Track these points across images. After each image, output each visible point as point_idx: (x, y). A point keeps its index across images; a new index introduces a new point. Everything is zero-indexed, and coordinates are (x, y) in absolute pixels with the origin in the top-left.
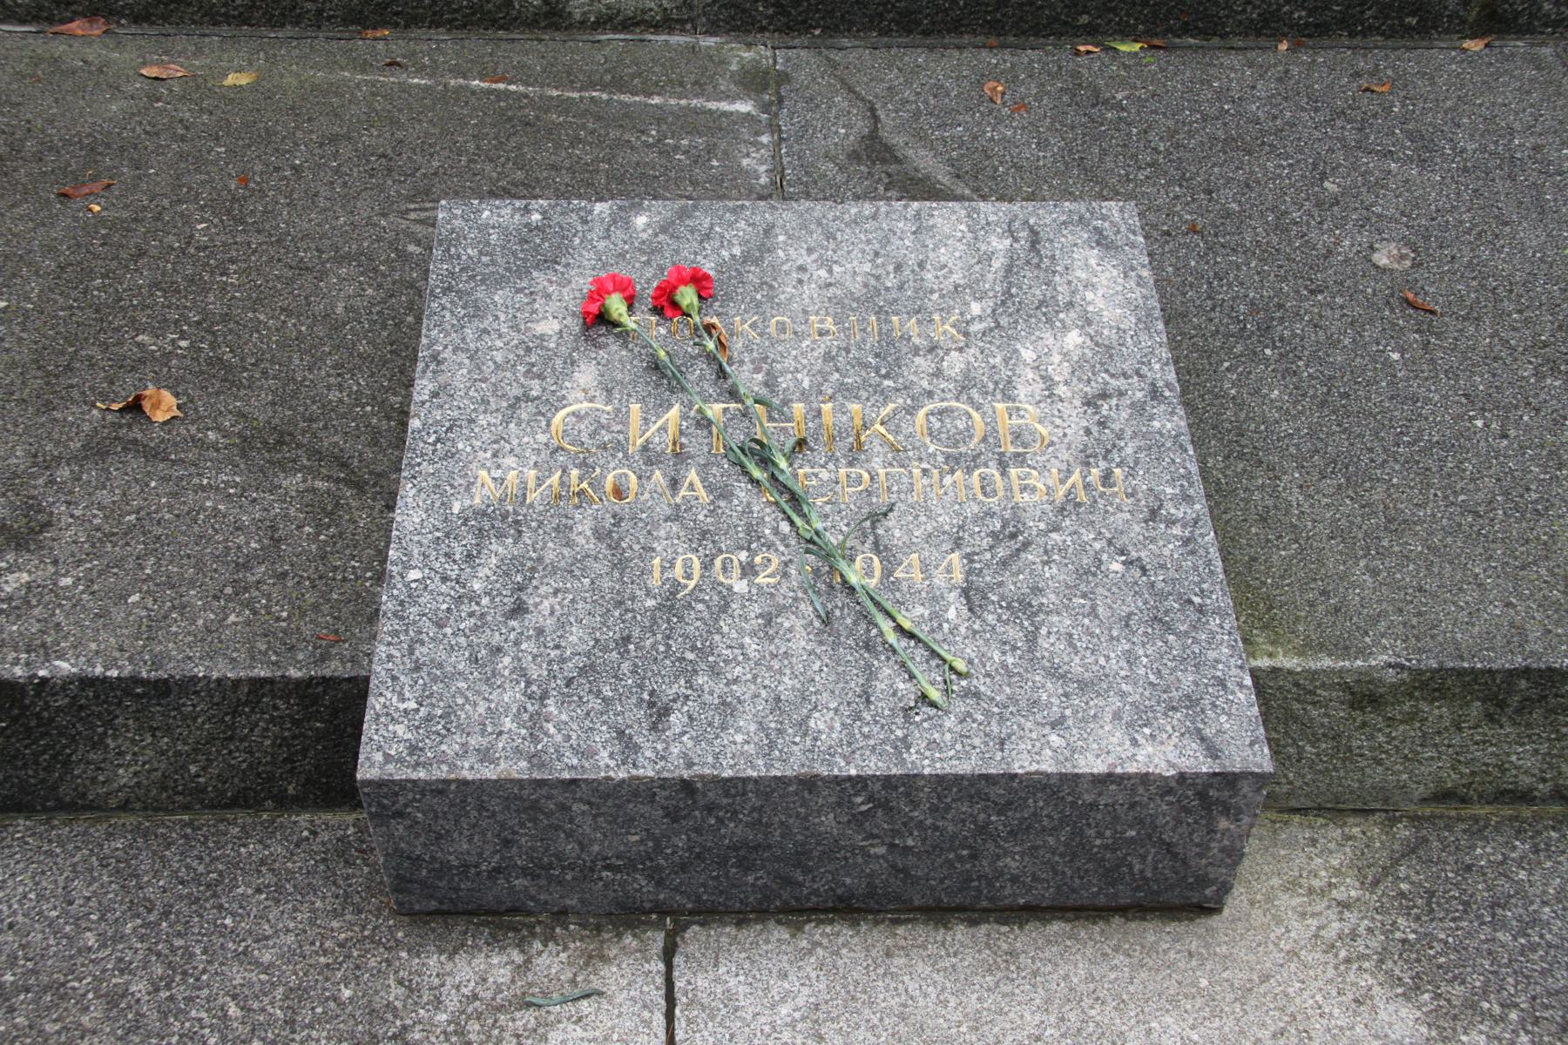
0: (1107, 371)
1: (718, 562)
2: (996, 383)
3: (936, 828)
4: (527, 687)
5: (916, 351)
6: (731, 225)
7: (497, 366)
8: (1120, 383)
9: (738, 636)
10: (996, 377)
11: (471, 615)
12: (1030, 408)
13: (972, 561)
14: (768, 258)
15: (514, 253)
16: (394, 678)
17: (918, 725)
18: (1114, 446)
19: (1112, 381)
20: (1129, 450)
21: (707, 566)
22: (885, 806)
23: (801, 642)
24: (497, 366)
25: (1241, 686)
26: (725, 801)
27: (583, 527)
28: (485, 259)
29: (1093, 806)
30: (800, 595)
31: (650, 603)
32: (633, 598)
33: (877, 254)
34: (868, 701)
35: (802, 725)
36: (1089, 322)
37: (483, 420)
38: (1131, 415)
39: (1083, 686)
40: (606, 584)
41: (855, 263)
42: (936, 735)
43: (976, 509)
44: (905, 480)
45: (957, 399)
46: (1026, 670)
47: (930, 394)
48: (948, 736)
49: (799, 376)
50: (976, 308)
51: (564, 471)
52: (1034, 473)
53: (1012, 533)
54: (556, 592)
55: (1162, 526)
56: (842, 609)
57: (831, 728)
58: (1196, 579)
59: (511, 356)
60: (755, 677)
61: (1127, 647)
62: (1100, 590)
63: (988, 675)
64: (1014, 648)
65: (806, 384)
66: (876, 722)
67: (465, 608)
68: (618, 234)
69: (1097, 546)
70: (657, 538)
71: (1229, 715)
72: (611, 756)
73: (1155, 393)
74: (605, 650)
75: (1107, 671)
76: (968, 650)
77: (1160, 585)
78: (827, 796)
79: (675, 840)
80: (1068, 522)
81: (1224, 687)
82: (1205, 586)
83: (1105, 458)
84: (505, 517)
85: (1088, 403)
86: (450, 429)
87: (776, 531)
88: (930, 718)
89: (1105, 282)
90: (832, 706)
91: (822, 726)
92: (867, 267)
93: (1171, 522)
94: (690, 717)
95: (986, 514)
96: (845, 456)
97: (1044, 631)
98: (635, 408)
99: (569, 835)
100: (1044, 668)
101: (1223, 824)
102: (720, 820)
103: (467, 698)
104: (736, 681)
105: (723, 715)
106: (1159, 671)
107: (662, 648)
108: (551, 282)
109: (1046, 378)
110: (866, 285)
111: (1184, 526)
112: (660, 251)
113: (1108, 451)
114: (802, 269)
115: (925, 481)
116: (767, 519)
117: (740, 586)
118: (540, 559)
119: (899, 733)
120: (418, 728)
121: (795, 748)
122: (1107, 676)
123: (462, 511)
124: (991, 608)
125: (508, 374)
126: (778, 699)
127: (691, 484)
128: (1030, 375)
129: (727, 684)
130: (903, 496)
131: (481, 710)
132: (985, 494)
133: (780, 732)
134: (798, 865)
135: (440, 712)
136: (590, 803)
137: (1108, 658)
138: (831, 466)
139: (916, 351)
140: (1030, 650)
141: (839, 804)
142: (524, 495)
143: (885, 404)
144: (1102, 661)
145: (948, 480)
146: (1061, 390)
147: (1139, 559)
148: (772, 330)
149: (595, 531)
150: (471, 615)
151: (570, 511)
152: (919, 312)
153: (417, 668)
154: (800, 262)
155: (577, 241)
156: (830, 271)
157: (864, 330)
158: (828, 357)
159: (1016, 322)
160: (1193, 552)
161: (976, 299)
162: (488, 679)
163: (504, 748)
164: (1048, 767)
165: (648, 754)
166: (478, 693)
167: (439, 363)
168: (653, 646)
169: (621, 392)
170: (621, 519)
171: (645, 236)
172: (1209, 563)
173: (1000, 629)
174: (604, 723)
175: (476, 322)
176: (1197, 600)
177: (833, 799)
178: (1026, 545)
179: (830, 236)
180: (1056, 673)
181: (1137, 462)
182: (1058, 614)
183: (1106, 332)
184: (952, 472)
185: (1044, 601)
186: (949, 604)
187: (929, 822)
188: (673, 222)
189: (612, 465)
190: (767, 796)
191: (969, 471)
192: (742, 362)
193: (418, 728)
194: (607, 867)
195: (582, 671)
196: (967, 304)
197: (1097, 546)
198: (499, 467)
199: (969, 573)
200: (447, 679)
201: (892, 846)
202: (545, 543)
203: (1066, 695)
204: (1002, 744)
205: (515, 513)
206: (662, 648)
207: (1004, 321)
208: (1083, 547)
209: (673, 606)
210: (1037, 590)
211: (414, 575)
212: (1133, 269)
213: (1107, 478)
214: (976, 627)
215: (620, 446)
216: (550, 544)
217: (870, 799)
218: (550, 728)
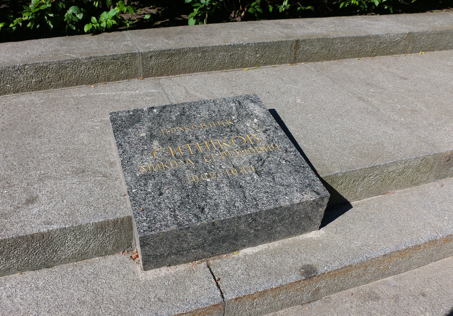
7: (135, 144)
11: (151, 197)
16: (139, 213)
23: (226, 189)
24: (135, 144)
31: (190, 187)
35: (234, 205)
37: (136, 156)
39: (288, 186)
48: (265, 202)
50: (233, 117)
53: (260, 159)
54: (168, 189)
60: (220, 198)
64: (271, 182)
65: (205, 137)
68: (151, 114)
69: (278, 159)
73: (276, 128)
74: (184, 198)
86: (129, 159)
92: (208, 113)
93: (290, 152)
102: (220, 231)
104: (216, 199)
105: (216, 206)
109: (254, 129)
115: (238, 152)
117: (208, 180)
118: (161, 182)
136: (191, 233)
141: (245, 221)
146: (258, 130)
149: (171, 174)
150: (151, 197)
151: (165, 171)
160: (297, 157)
164: (288, 203)
165: (203, 218)
166: (159, 213)
168: (195, 195)
178: (264, 161)
192: (189, 135)
195: (181, 204)
197: (278, 159)
199: (255, 169)
200: (151, 211)
207: (240, 119)
208: (276, 160)
210: (271, 170)
211: (134, 191)
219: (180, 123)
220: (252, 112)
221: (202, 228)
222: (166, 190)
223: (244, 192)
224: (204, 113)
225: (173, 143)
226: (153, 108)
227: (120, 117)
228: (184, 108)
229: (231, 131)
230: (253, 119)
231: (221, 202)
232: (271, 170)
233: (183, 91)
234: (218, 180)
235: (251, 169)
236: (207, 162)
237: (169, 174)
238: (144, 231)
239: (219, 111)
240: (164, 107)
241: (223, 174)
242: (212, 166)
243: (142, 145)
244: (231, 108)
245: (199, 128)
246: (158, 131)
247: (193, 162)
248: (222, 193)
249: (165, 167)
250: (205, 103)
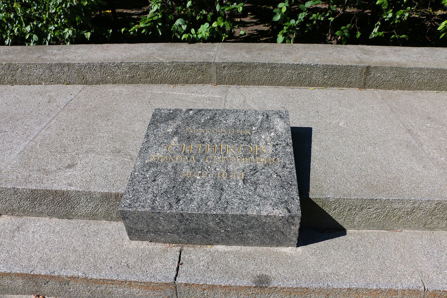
3: (234, 227)
7: (159, 137)
8: (281, 142)
9: (196, 187)
14: (214, 119)
16: (129, 192)
22: (222, 221)
23: (208, 188)
24: (159, 137)
25: (297, 199)
26: (190, 218)
27: (170, 166)
29: (265, 222)
31: (180, 180)
32: (177, 179)
35: (206, 204)
39: (264, 198)
40: (172, 176)
50: (254, 128)
53: (255, 170)
64: (252, 191)
68: (187, 114)
73: (287, 144)
74: (170, 188)
78: (210, 218)
79: (181, 227)
81: (294, 199)
84: (155, 164)
87: (207, 168)
92: (234, 121)
93: (287, 168)
102: (189, 223)
114: (221, 121)
115: (239, 159)
117: (198, 178)
118: (160, 171)
131: (144, 198)
134: (207, 234)
137: (270, 193)
146: (269, 143)
149: (172, 167)
151: (168, 163)
153: (133, 190)
158: (223, 136)
164: (255, 213)
172: (294, 176)
176: (290, 183)
177: (212, 219)
180: (260, 196)
187: (232, 225)
192: (206, 137)
194: (168, 232)
195: (165, 192)
201: (225, 230)
203: (261, 200)
204: (246, 209)
207: (259, 131)
210: (258, 180)
217: (219, 219)
219: (205, 126)
221: (172, 216)
223: (221, 194)
224: (231, 120)
226: (191, 110)
229: (245, 140)
230: (271, 132)
232: (258, 180)
233: (242, 100)
235: (241, 176)
236: (207, 163)
238: (125, 206)
239: (244, 120)
240: (200, 111)
241: (214, 175)
242: (209, 167)
245: (218, 133)
248: (203, 191)
249: (171, 160)
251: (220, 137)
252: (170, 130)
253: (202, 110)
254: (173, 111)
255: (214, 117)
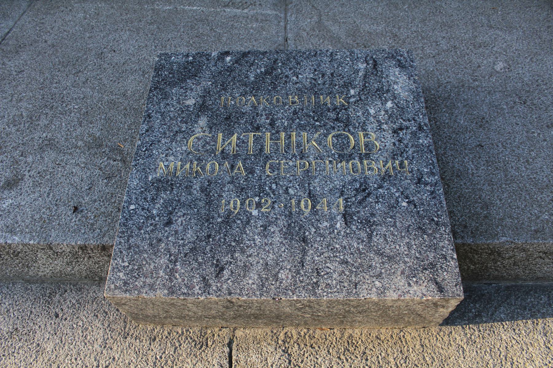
0: (402, 118)
1: (247, 202)
2: (359, 123)
3: (329, 311)
4: (170, 257)
5: (329, 110)
6: (261, 59)
7: (171, 119)
10: (359, 121)
11: (151, 225)
12: (372, 134)
13: (347, 202)
15: (181, 73)
17: (322, 276)
18: (404, 150)
19: (404, 123)
20: (410, 152)
21: (242, 204)
23: (277, 238)
24: (171, 119)
25: (452, 258)
28: (171, 75)
29: (392, 306)
30: (278, 217)
32: (213, 218)
33: (315, 70)
34: (303, 266)
36: (395, 98)
38: (411, 137)
39: (390, 258)
41: (307, 74)
42: (330, 281)
43: (350, 178)
44: (322, 165)
45: (344, 131)
46: (367, 252)
47: (334, 128)
48: (334, 282)
49: (283, 121)
51: (191, 162)
52: (373, 162)
53: (364, 189)
55: (423, 186)
56: (294, 223)
57: (287, 277)
58: (436, 210)
59: (176, 114)
60: (258, 254)
61: (408, 241)
62: (398, 215)
63: (352, 254)
64: (363, 241)
65: (286, 124)
66: (305, 275)
67: (150, 222)
68: (220, 64)
70: (224, 191)
71: (447, 272)
72: (200, 289)
73: (420, 128)
74: (201, 241)
75: (399, 252)
76: (344, 242)
77: (421, 212)
80: (386, 184)
81: (446, 259)
82: (439, 213)
83: (401, 156)
84: (167, 182)
85: (395, 132)
86: (151, 145)
87: (270, 188)
88: (328, 273)
89: (401, 82)
90: (288, 267)
91: (284, 277)
92: (312, 76)
93: (426, 184)
94: (232, 272)
95: (354, 180)
96: (299, 155)
97: (375, 234)
98: (220, 135)
99: (189, 311)
100: (374, 251)
101: (441, 310)
103: (147, 261)
105: (245, 271)
106: (420, 252)
107: (222, 240)
108: (193, 84)
109: (379, 121)
110: (311, 83)
111: (431, 186)
112: (234, 70)
113: (402, 153)
115: (330, 166)
116: (267, 183)
117: (255, 213)
118: (179, 200)
119: (315, 280)
120: (128, 274)
121: (272, 287)
122: (399, 254)
123: (152, 180)
124: (354, 223)
125: (174, 122)
126: (267, 264)
127: (239, 168)
128: (373, 120)
129: (247, 257)
130: (321, 172)
131: (152, 267)
132: (354, 172)
133: (267, 279)
135: (136, 267)
137: (400, 246)
138: (294, 159)
139: (329, 110)
140: (369, 242)
142: (176, 172)
143: (316, 132)
144: (398, 247)
145: (339, 165)
146: (385, 126)
147: (413, 200)
148: (274, 101)
149: (201, 188)
150: (151, 225)
152: (331, 93)
153: (129, 248)
154: (286, 74)
155: (204, 67)
156: (297, 77)
157: (309, 101)
158: (295, 113)
159: (368, 98)
160: (434, 198)
161: (353, 88)
162: (156, 253)
163: (159, 284)
165: (214, 288)
166: (151, 259)
167: (150, 118)
169: (215, 129)
170: (211, 183)
171: (229, 65)
172: (441, 203)
173: (357, 233)
174: (198, 273)
175: (165, 101)
176: (436, 219)
178: (369, 194)
179: (298, 63)
181: (413, 157)
182: (381, 226)
183: (402, 102)
184: (341, 162)
185: (375, 220)
186: (337, 221)
187: (327, 310)
188: (240, 59)
189: (209, 159)
190: (262, 304)
191: (348, 162)
192: (262, 115)
193: (128, 274)
195: (191, 250)
196: (349, 90)
197: (397, 195)
198: (167, 161)
199: (346, 207)
202: (181, 193)
204: (356, 286)
205: (172, 180)
206: (222, 240)
209: (228, 221)
210: (373, 215)
211: (132, 207)
212: (412, 76)
213: (401, 165)
214: (348, 231)
215: (213, 151)
216: (183, 194)
218: (177, 275)
219: (258, 89)
220: (390, 86)
222: (180, 217)
223: (304, 252)
224: (306, 75)
225: (229, 125)
226: (227, 53)
227: (171, 64)
228: (275, 61)
229: (337, 119)
230: (386, 101)
231: (258, 263)
232: (373, 215)
233: (315, 18)
234: (270, 218)
236: (268, 176)
237: (197, 187)
241: (285, 206)
242: (274, 186)
243: (181, 122)
244: (357, 71)
245: (285, 104)
246: (216, 99)
247: (246, 171)
248: (266, 244)
250: (315, 55)
251: (289, 113)
252: (191, 102)
253: (249, 52)
254: (193, 57)
255: (273, 69)
